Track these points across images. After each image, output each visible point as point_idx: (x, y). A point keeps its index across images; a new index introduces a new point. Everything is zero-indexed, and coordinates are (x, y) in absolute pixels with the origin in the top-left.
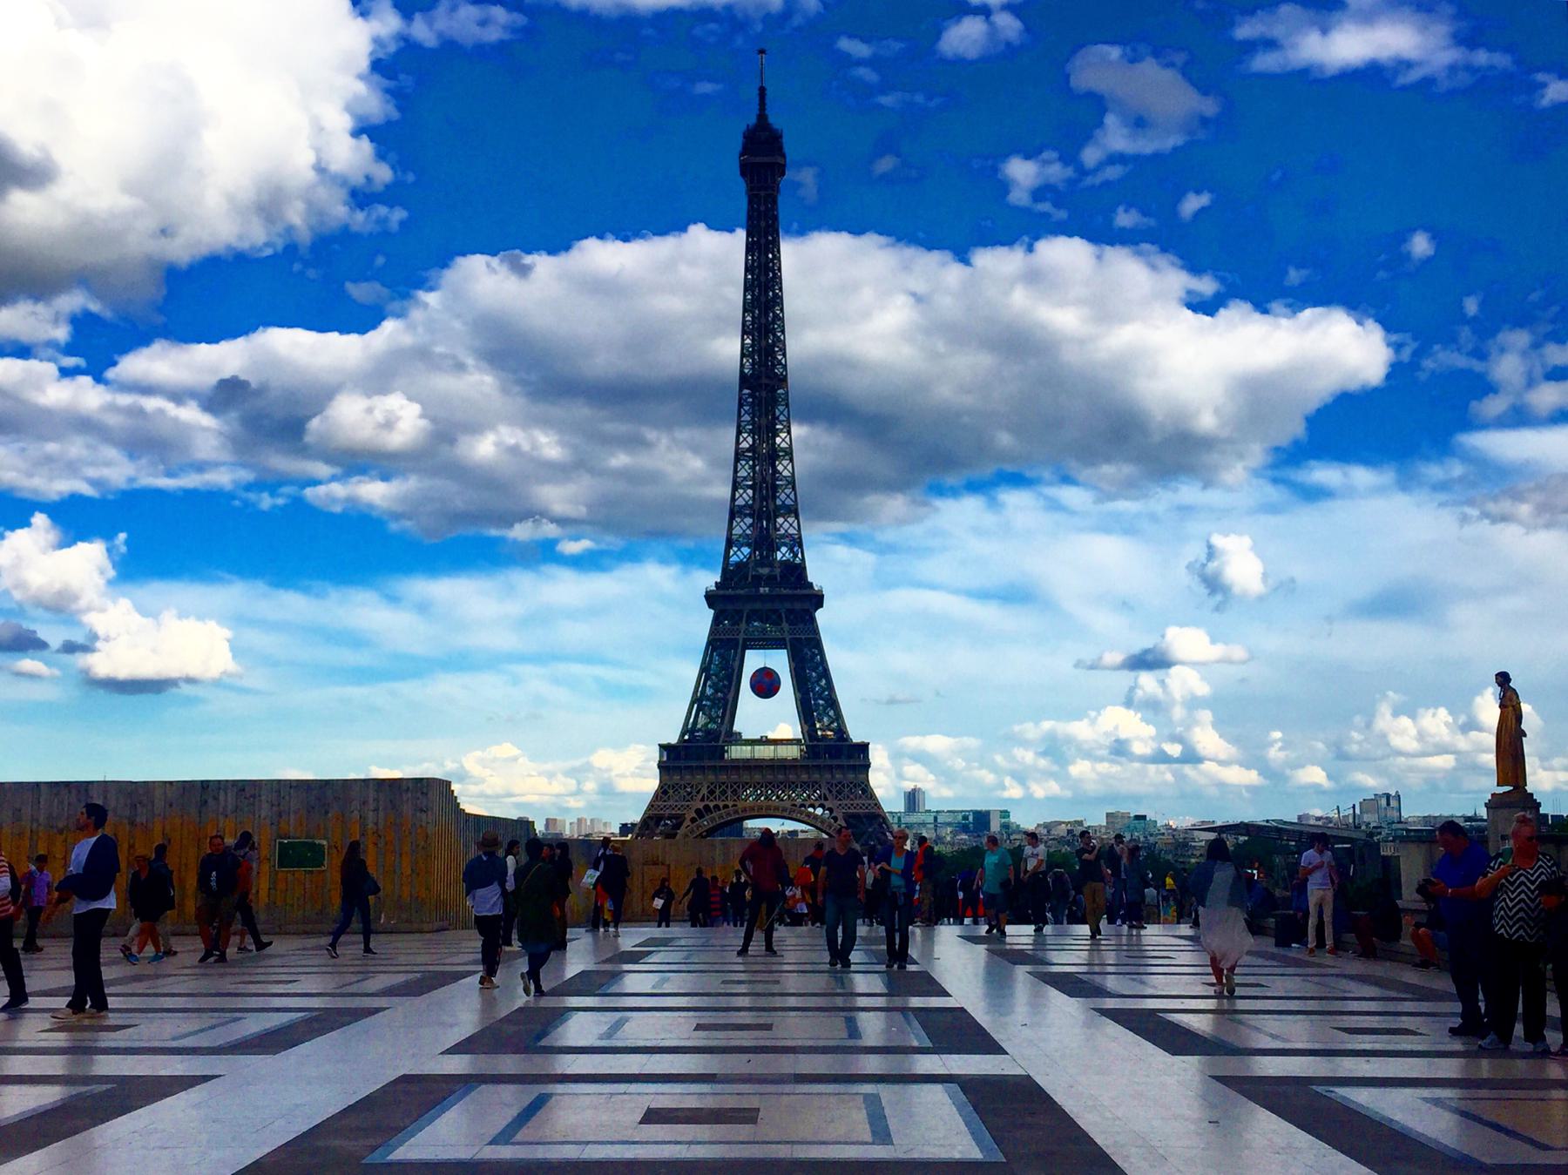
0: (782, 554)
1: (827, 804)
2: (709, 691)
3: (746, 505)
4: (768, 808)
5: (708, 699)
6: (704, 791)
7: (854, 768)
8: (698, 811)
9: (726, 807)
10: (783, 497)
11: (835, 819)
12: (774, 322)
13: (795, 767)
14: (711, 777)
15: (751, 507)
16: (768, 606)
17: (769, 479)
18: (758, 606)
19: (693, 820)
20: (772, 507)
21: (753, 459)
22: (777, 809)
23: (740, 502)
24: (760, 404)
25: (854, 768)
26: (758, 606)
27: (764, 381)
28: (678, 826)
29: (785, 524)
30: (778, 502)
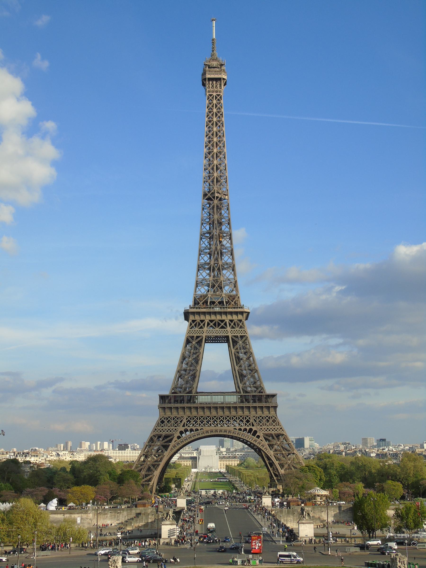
0: (227, 289)
1: (254, 429)
2: (184, 366)
3: (206, 263)
4: (221, 431)
5: (185, 370)
6: (185, 421)
7: (268, 408)
8: (181, 433)
9: (197, 430)
10: (226, 259)
11: (258, 437)
12: (220, 164)
13: (236, 408)
14: (188, 413)
15: (209, 264)
16: (219, 317)
17: (219, 248)
18: (213, 317)
19: (179, 437)
20: (220, 263)
21: (210, 238)
22: (225, 431)
23: (202, 261)
24: (213, 207)
25: (268, 408)
26: (213, 317)
27: (216, 195)
28: (170, 441)
29: (227, 274)
30: (223, 261)
